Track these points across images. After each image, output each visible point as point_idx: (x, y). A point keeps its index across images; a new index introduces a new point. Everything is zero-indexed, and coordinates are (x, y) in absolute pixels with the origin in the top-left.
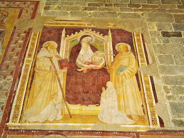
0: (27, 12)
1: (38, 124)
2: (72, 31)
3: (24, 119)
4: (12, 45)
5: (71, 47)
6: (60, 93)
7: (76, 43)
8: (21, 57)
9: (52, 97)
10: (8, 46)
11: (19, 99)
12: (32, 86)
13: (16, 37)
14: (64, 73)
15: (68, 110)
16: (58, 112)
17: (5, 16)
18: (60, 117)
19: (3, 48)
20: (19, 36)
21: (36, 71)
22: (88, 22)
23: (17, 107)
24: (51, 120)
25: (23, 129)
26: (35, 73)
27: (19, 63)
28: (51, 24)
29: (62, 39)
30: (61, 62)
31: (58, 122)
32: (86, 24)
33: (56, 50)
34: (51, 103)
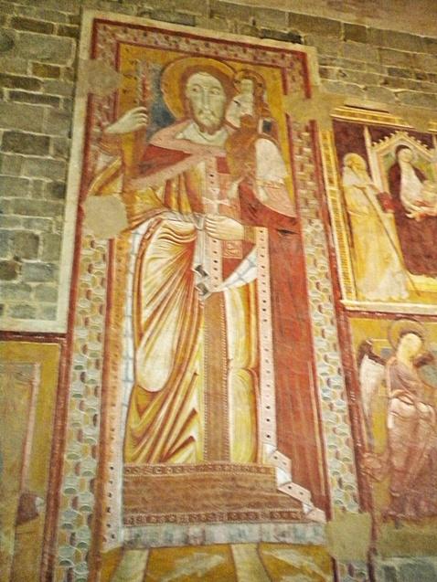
0: (294, 80)
1: (381, 303)
2: (380, 134)
3: (360, 294)
4: (298, 158)
5: (388, 168)
6: (395, 255)
7: (391, 161)
8: (319, 185)
9: (386, 261)
10: (292, 160)
11: (344, 262)
12: (355, 241)
13: (297, 141)
14: (391, 219)
15: (413, 284)
16: (400, 286)
17: (260, 85)
18: (406, 295)
19: (286, 163)
20: (300, 137)
21: (350, 213)
22: (398, 115)
23: (345, 274)
24: (395, 298)
25: (363, 309)
26: (351, 218)
27: (321, 197)
28: (342, 113)
29: (369, 150)
30: (380, 197)
31: (404, 301)
32: (396, 118)
33: (367, 176)
34: (387, 271)
